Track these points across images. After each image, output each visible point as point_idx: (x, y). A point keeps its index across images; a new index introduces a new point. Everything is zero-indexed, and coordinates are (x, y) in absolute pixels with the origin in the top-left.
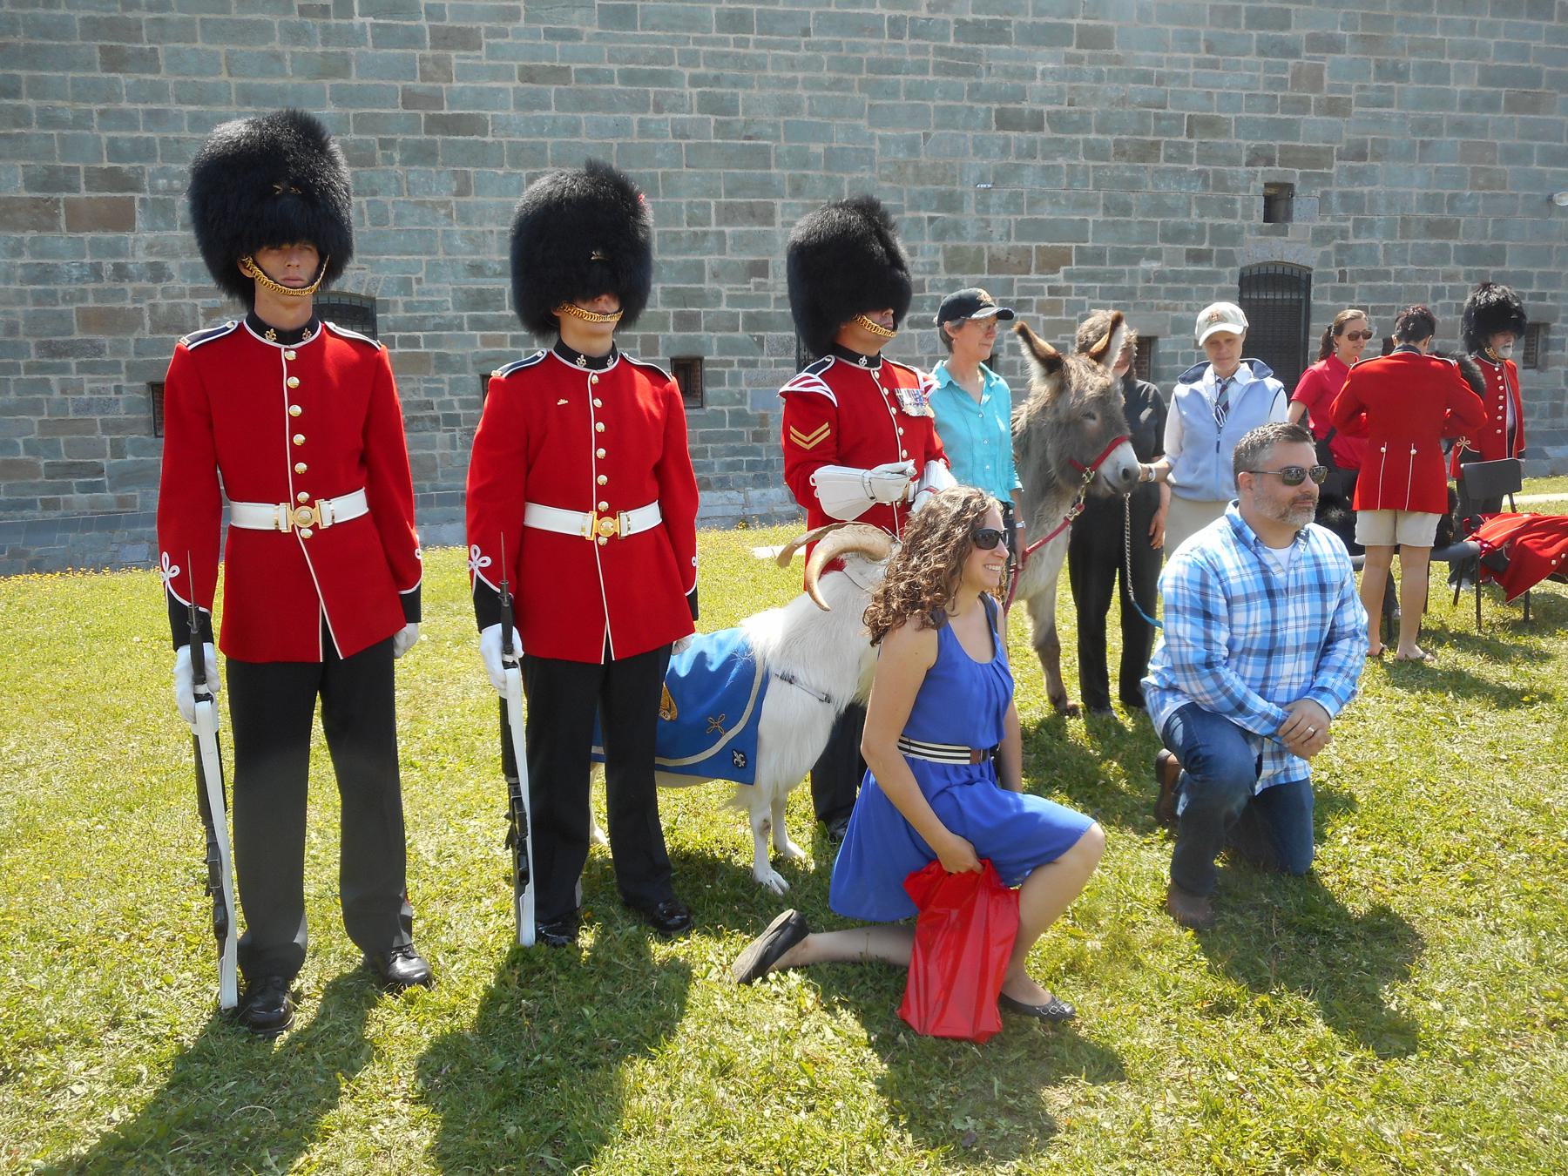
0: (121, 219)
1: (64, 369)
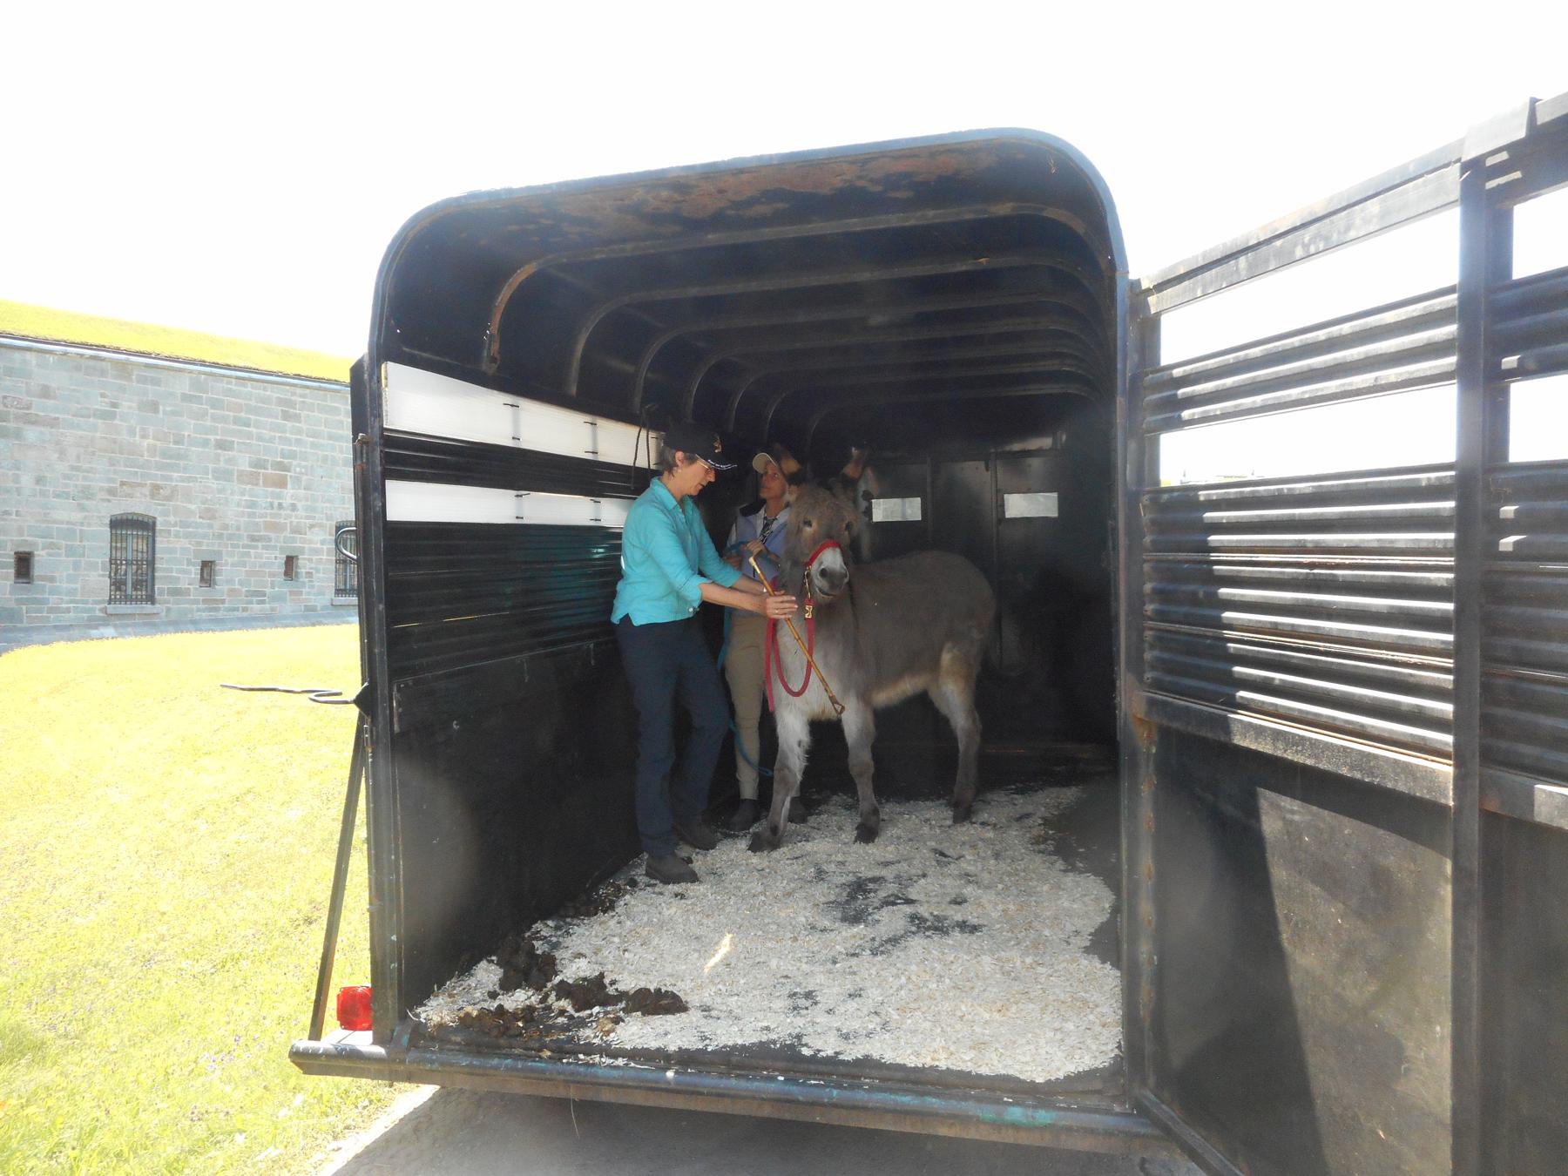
0: (282, 483)
1: (256, 547)
